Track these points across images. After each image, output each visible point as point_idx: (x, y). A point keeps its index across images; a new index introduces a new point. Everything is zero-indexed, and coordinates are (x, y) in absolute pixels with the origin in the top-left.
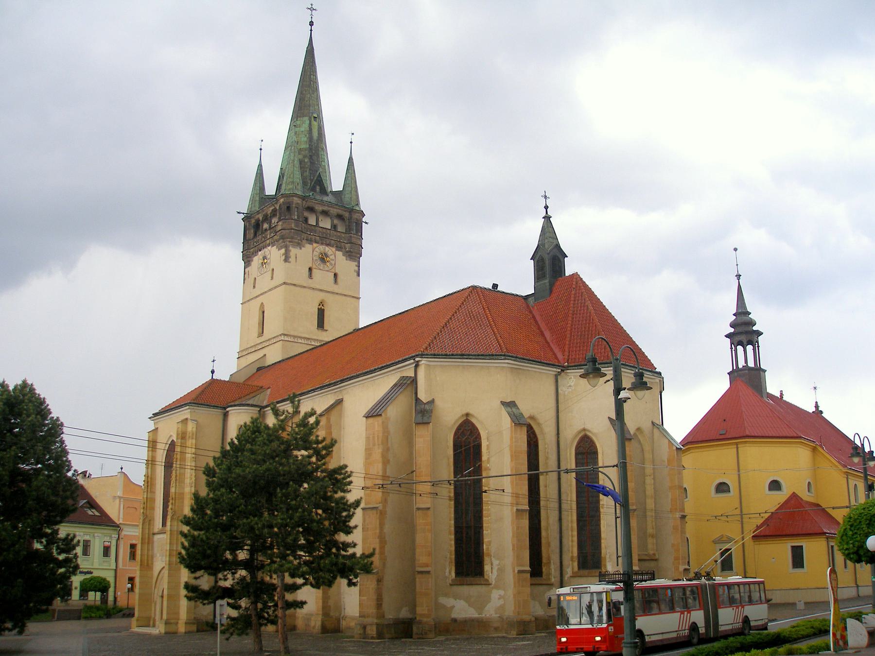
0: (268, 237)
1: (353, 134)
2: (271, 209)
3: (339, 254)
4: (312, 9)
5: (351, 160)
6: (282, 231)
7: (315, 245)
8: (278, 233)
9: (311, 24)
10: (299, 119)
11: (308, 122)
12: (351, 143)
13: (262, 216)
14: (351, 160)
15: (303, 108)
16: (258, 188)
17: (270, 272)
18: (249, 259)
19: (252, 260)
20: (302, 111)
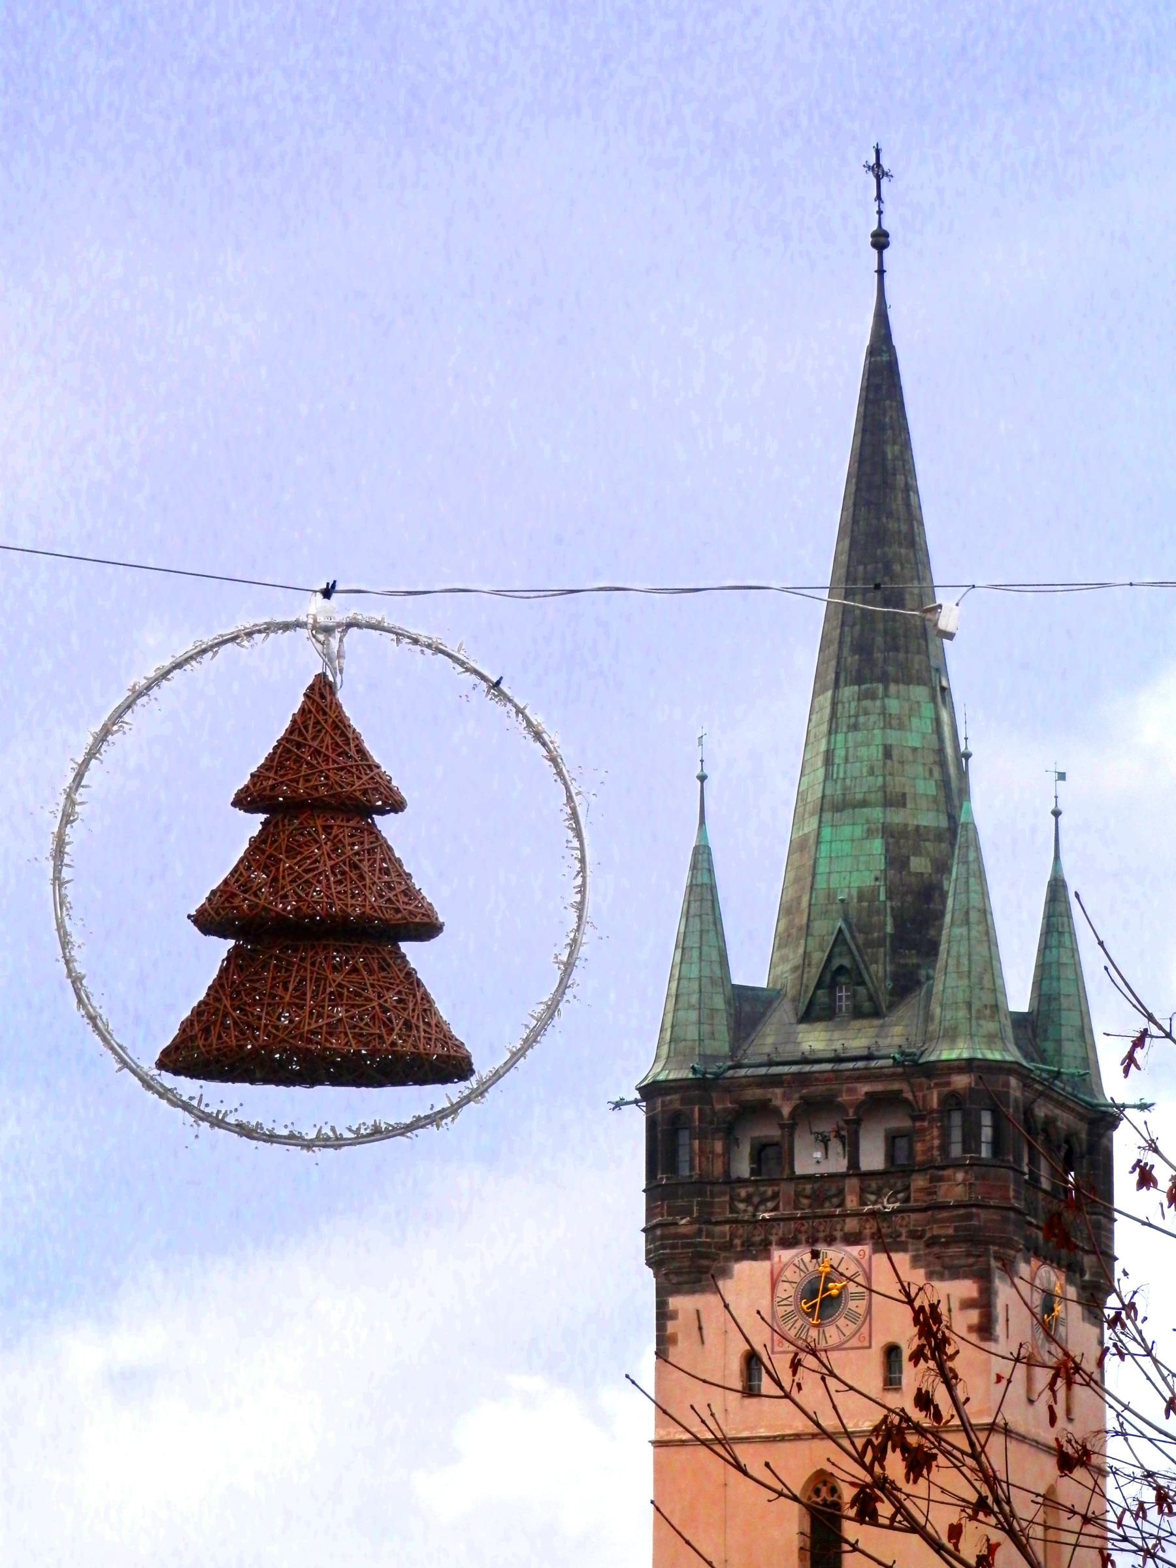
0: (851, 1202)
1: (1062, 776)
2: (864, 1088)
3: (1072, 1292)
4: (878, 171)
5: (1057, 890)
6: (974, 1210)
7: (1034, 1261)
8: (945, 1214)
9: (880, 240)
10: (893, 688)
11: (927, 710)
12: (1056, 813)
13: (794, 1102)
14: (1057, 890)
15: (902, 642)
16: (715, 956)
17: (875, 1357)
18: (705, 1262)
19: (725, 1273)
20: (901, 656)
